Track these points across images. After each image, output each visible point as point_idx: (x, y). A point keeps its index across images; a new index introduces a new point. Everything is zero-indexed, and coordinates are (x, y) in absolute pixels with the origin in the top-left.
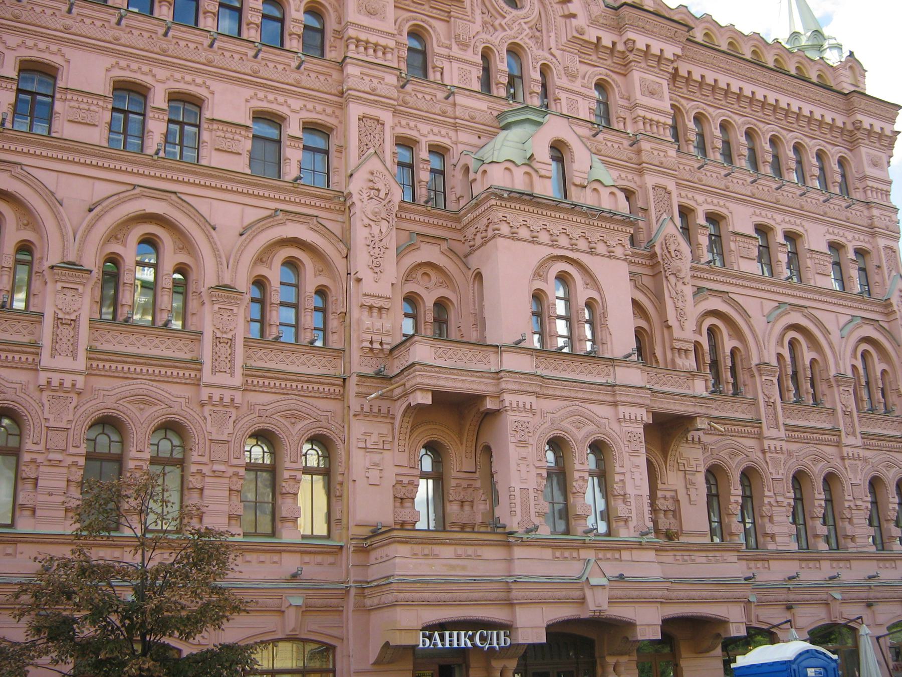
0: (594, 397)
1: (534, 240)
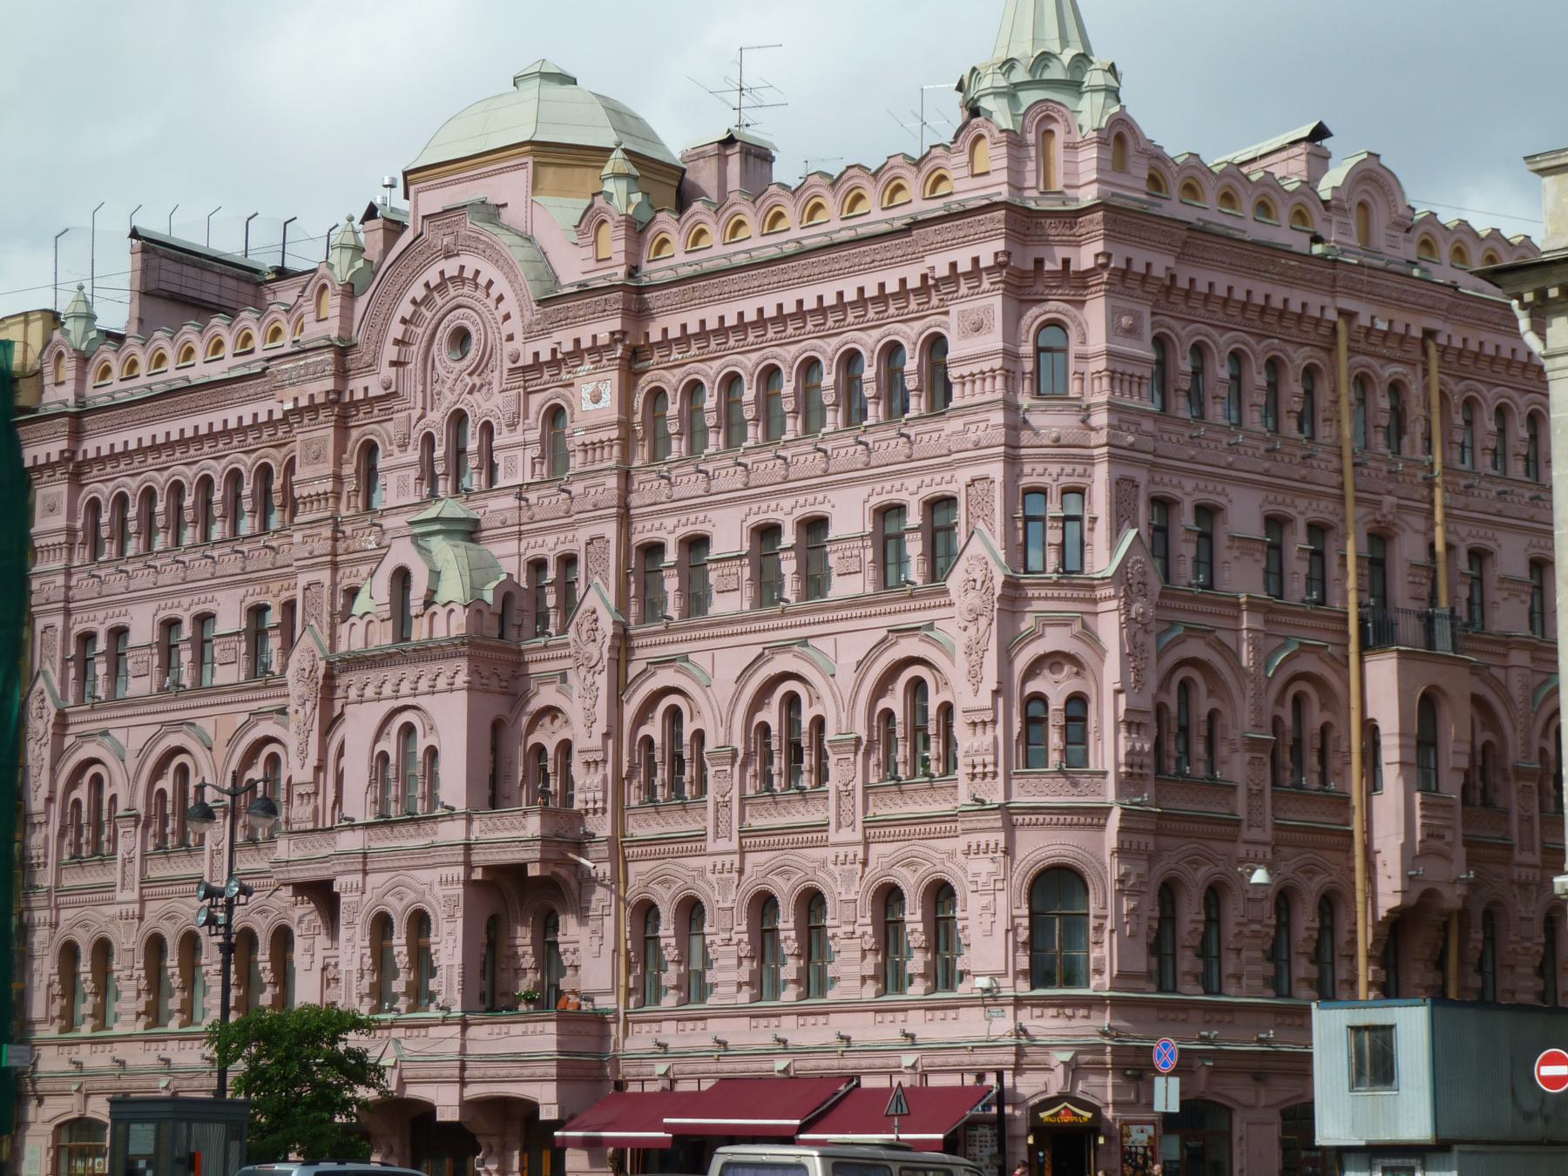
0: (416, 862)
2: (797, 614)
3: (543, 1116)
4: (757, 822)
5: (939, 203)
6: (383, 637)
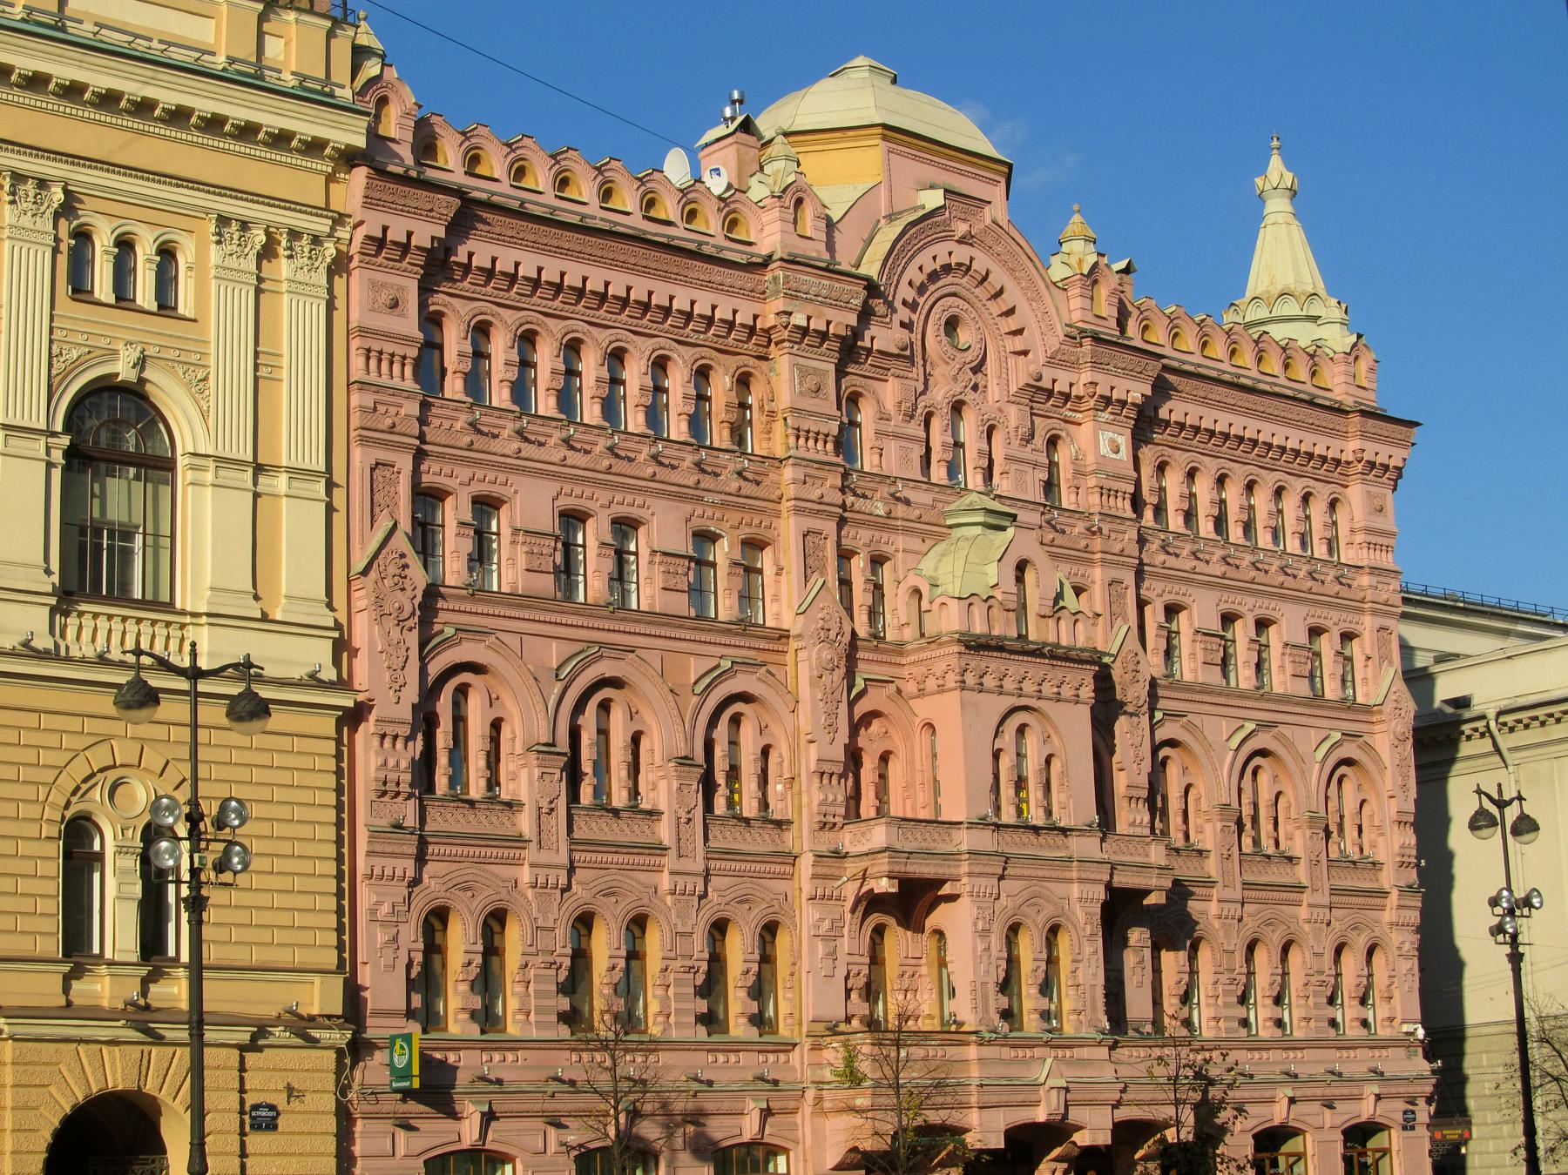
1: (1000, 691)
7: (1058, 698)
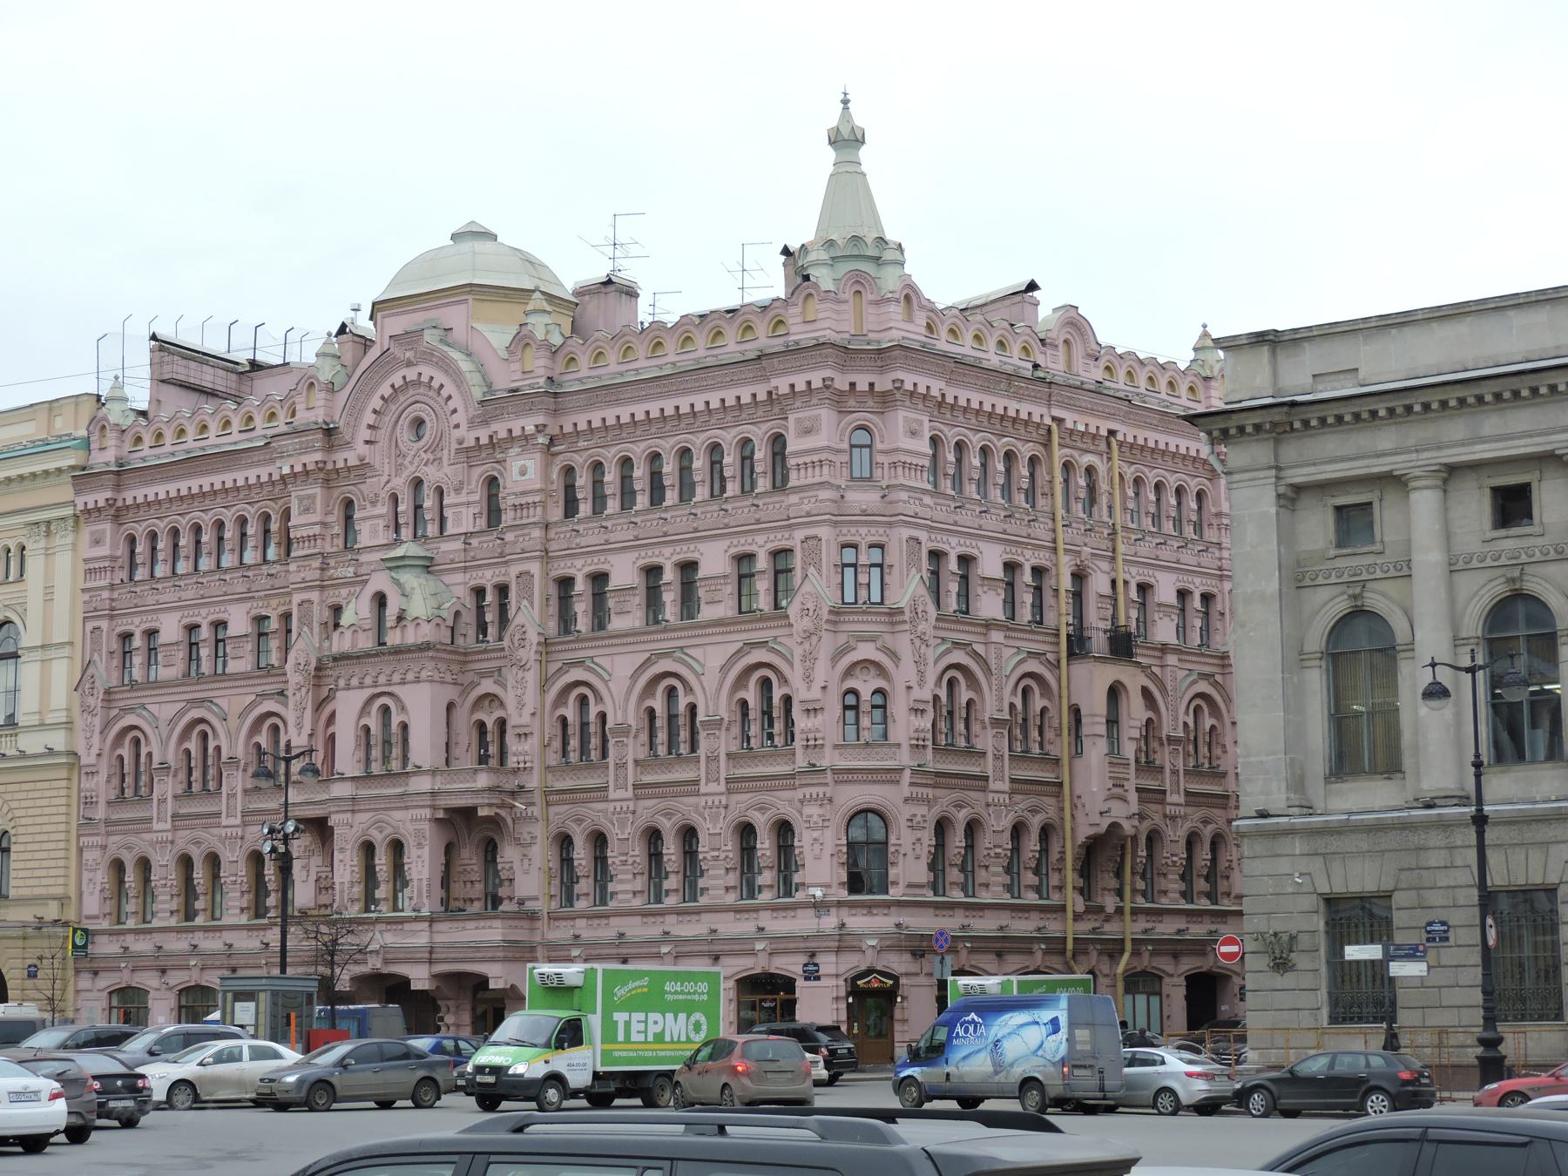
2: (675, 630)
3: (492, 986)
4: (647, 779)
5: (781, 340)
6: (366, 642)
7: (403, 682)
